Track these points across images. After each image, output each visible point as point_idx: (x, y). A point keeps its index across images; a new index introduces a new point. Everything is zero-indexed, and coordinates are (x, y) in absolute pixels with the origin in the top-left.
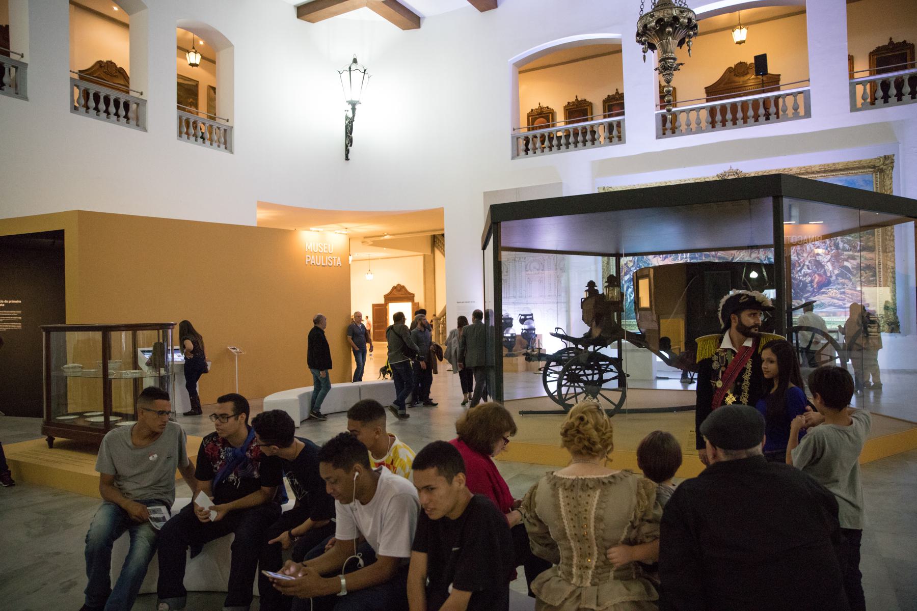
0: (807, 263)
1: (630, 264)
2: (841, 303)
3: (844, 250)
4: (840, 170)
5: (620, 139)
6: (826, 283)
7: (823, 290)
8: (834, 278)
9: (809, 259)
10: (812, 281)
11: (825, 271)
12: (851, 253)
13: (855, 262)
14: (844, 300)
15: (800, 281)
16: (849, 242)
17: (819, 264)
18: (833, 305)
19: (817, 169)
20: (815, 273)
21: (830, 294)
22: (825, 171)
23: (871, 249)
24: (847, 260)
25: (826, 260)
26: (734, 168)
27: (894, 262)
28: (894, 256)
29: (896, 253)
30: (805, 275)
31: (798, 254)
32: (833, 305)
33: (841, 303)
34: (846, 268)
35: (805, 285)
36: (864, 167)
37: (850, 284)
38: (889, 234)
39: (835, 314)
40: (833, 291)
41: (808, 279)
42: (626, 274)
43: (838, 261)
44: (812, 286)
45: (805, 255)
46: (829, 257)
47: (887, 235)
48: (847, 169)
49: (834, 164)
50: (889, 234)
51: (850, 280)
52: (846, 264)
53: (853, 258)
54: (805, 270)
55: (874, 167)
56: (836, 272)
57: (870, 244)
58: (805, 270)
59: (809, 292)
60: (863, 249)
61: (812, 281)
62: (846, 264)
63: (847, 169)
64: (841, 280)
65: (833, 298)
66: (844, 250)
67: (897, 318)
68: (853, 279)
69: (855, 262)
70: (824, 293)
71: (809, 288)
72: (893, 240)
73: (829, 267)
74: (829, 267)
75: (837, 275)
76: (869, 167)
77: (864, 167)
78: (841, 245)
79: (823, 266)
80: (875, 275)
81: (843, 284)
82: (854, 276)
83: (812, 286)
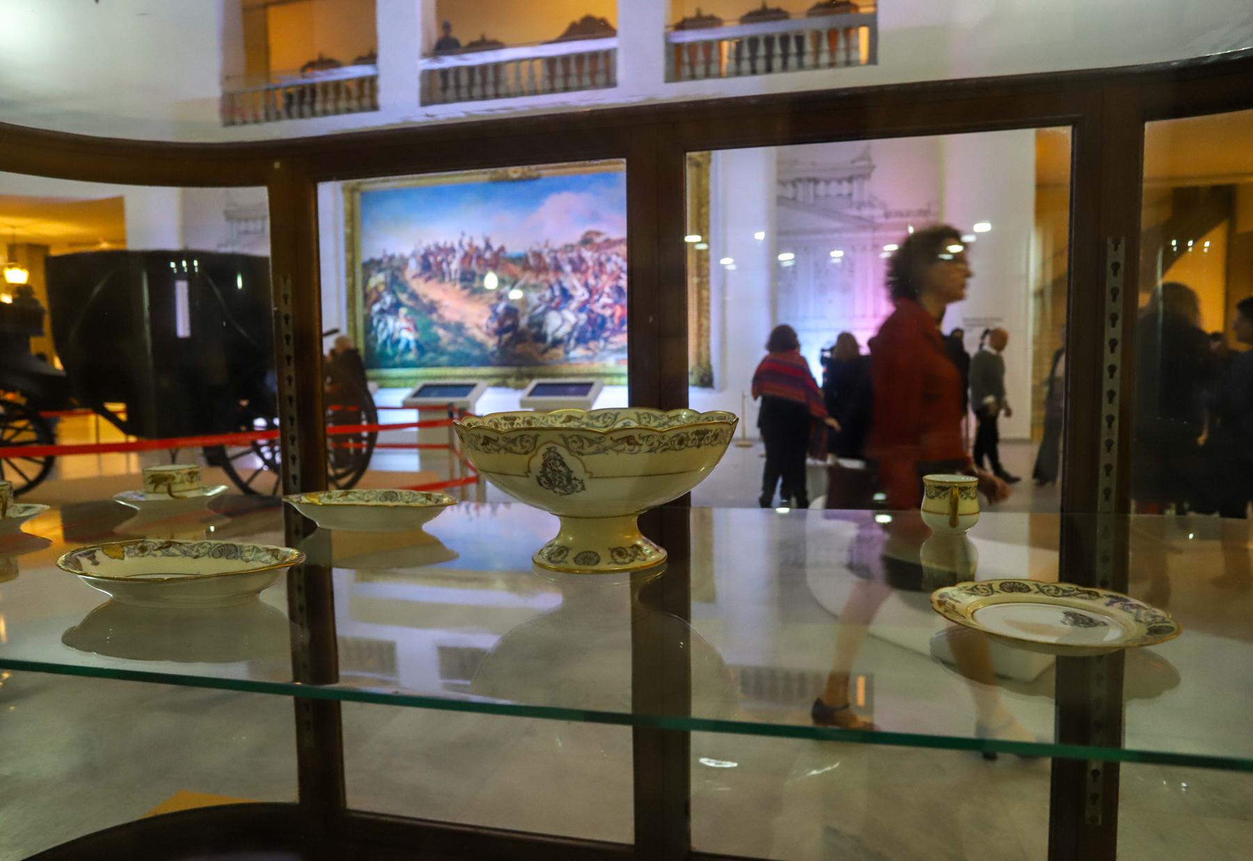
1: (382, 288)
15: (598, 315)
30: (604, 307)
31: (596, 277)
35: (604, 319)
41: (608, 312)
42: (375, 302)
45: (604, 277)
54: (605, 300)
58: (605, 300)
61: (612, 316)
71: (609, 325)
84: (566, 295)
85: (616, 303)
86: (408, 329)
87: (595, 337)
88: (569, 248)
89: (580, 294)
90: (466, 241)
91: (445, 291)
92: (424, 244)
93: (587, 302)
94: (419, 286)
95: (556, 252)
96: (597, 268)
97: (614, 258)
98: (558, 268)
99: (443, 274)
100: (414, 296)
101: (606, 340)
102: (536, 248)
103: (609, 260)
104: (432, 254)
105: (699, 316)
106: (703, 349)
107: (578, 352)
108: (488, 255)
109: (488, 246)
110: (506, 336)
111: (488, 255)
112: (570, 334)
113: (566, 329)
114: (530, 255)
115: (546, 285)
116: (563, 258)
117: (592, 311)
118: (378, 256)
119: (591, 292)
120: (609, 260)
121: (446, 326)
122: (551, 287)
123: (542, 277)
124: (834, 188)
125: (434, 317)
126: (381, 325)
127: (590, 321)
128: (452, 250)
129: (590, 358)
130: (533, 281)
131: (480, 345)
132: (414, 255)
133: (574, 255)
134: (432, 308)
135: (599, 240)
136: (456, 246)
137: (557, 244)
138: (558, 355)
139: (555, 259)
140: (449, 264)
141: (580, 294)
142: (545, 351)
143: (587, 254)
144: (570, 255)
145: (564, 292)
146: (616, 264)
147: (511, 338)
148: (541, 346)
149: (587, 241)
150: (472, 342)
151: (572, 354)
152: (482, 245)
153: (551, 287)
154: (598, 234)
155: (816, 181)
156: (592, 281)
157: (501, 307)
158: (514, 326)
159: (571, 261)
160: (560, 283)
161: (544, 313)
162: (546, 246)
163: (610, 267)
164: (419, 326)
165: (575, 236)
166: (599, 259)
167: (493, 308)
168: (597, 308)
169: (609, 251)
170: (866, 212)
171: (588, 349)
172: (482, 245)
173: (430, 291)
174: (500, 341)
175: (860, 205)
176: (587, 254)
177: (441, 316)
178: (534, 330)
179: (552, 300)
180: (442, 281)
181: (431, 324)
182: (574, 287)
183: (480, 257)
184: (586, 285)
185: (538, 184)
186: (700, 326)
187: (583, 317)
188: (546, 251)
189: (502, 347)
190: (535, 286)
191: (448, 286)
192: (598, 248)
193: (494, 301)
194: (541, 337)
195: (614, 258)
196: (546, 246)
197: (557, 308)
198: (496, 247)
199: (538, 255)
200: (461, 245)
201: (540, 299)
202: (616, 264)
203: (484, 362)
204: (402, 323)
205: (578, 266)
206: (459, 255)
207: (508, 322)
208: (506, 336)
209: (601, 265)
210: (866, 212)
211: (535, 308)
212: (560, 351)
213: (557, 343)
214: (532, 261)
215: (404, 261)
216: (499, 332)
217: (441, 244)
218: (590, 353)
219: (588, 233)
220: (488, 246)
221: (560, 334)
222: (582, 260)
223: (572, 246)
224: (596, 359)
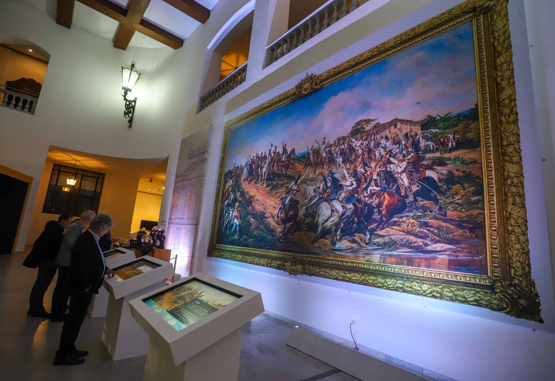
0: (375, 177)
2: (420, 242)
3: (427, 150)
4: (422, 33)
6: (398, 208)
7: (395, 219)
8: (411, 198)
9: (378, 170)
10: (380, 205)
11: (398, 188)
12: (438, 155)
13: (444, 170)
14: (424, 237)
15: (366, 204)
16: (434, 138)
17: (390, 178)
18: (408, 245)
19: (392, 43)
20: (384, 190)
21: (404, 226)
22: (402, 43)
23: (471, 144)
24: (430, 168)
25: (400, 170)
26: (310, 74)
27: (519, 163)
28: (518, 151)
29: (523, 145)
30: (371, 195)
31: (365, 165)
32: (408, 245)
33: (420, 242)
34: (430, 180)
36: (457, 16)
37: (436, 209)
38: (507, 111)
39: (410, 262)
40: (408, 220)
41: (375, 201)
43: (418, 171)
44: (380, 213)
46: (404, 165)
47: (502, 113)
48: (431, 29)
49: (413, 29)
50: (507, 111)
51: (436, 202)
52: (429, 173)
53: (441, 163)
54: (373, 188)
55: (474, 9)
56: (415, 188)
57: (471, 135)
58: (373, 188)
59: (375, 221)
60: (459, 145)
61: (380, 205)
62: (429, 173)
63: (431, 29)
64: (422, 202)
65: (408, 233)
66: (427, 150)
67: (532, 284)
68: (442, 200)
69: (444, 170)
70: (395, 224)
71: (376, 216)
72: (516, 121)
74: (405, 180)
75: (416, 194)
76: (465, 13)
77: (457, 16)
78: (423, 143)
79: (395, 180)
80: (479, 192)
81: (425, 209)
82: (443, 193)
83: (380, 213)
84: (337, 186)
85: (384, 190)
87: (361, 230)
89: (349, 183)
90: (273, 149)
93: (355, 191)
96: (366, 156)
97: (383, 142)
98: (332, 161)
100: (243, 194)
101: (372, 232)
102: (316, 146)
103: (378, 145)
105: (503, 203)
106: (515, 250)
107: (344, 244)
109: (285, 150)
110: (288, 225)
112: (337, 224)
113: (335, 219)
115: (321, 178)
117: (359, 201)
118: (232, 168)
119: (359, 181)
120: (378, 145)
121: (254, 216)
122: (325, 180)
126: (227, 214)
127: (356, 212)
129: (354, 251)
130: (311, 176)
131: (272, 231)
132: (246, 165)
135: (368, 128)
138: (325, 245)
139: (330, 152)
140: (262, 168)
141: (349, 183)
142: (316, 240)
144: (342, 147)
145: (335, 181)
146: (385, 148)
147: (292, 226)
148: (312, 234)
149: (357, 131)
150: (267, 226)
151: (338, 246)
154: (368, 121)
156: (360, 170)
158: (295, 215)
159: (343, 153)
160: (333, 174)
161: (317, 204)
162: (324, 143)
165: (347, 128)
167: (283, 199)
168: (364, 197)
169: (378, 137)
171: (354, 241)
174: (285, 229)
176: (356, 144)
177: (253, 208)
178: (308, 221)
179: (325, 191)
182: (344, 177)
183: (279, 160)
184: (355, 174)
185: (322, 92)
186: (505, 218)
187: (350, 206)
189: (285, 233)
190: (312, 180)
193: (284, 196)
194: (313, 227)
195: (383, 142)
196: (324, 143)
197: (329, 200)
199: (317, 152)
200: (270, 153)
201: (315, 191)
202: (385, 148)
203: (272, 246)
204: (235, 214)
205: (348, 156)
207: (291, 213)
208: (288, 225)
209: (370, 151)
211: (311, 200)
212: (328, 242)
213: (326, 232)
215: (242, 169)
216: (284, 221)
218: (354, 245)
219: (358, 123)
220: (285, 150)
221: (329, 224)
222: (352, 149)
223: (344, 138)
224: (361, 254)
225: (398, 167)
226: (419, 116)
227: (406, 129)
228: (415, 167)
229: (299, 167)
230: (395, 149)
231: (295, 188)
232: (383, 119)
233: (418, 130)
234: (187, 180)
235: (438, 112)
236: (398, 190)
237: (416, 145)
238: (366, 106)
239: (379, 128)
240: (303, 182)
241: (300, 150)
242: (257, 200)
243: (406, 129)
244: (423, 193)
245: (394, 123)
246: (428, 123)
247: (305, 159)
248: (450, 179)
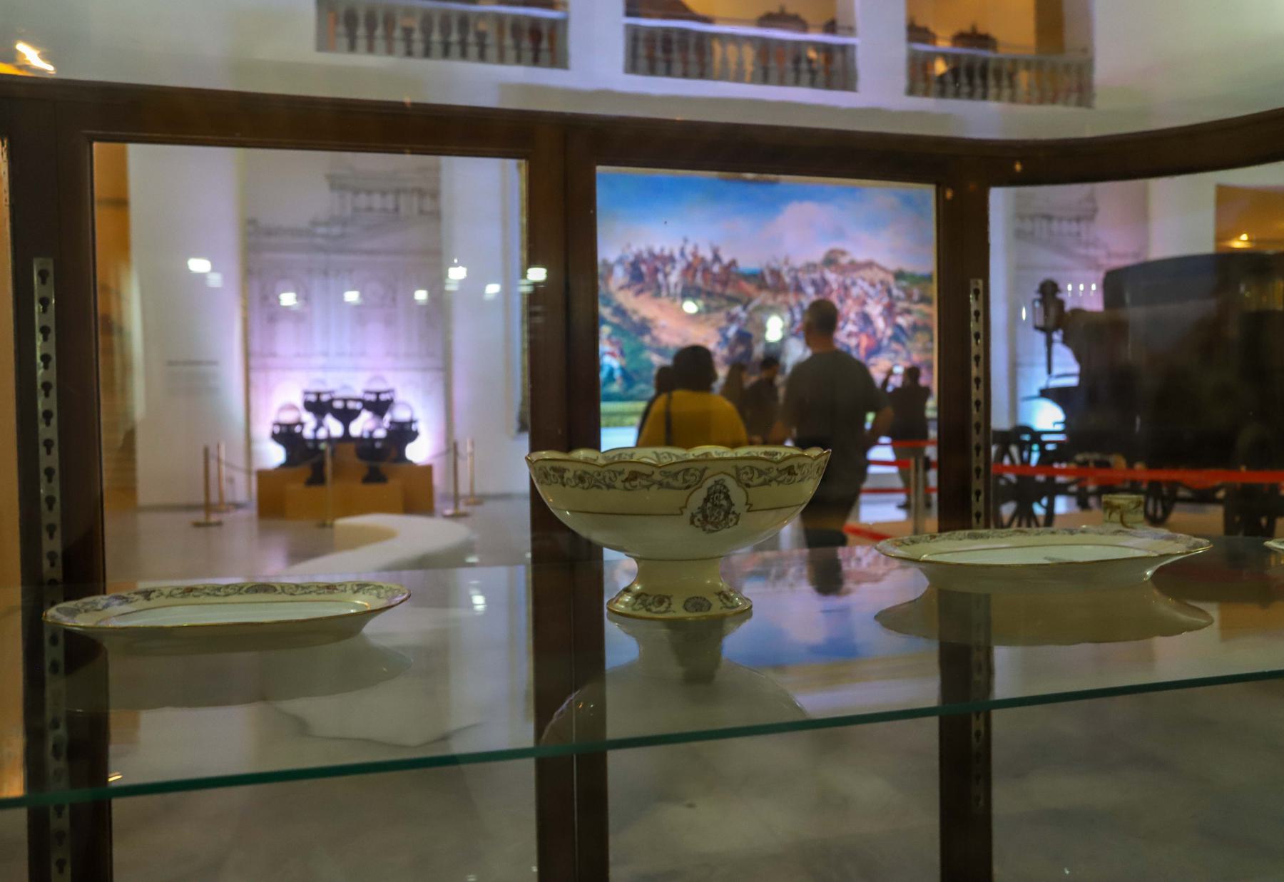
3: (898, 299)
5: (558, 59)
16: (904, 289)
17: (866, 319)
30: (850, 335)
34: (899, 327)
45: (849, 302)
51: (903, 344)
53: (907, 312)
54: (851, 327)
58: (851, 327)
61: (858, 346)
64: (894, 346)
68: (909, 345)
73: (880, 323)
74: (880, 323)
78: (895, 292)
85: (861, 331)
86: (612, 354)
88: (811, 267)
90: (689, 249)
91: (661, 307)
92: (635, 249)
94: (627, 299)
95: (797, 270)
96: (842, 292)
97: (860, 282)
99: (659, 287)
100: (620, 311)
102: (774, 265)
103: (854, 283)
104: (644, 261)
108: (716, 268)
109: (717, 258)
111: (716, 268)
114: (767, 273)
116: (805, 278)
120: (854, 283)
123: (780, 298)
124: (1067, 227)
125: (647, 339)
128: (671, 259)
132: (620, 261)
133: (816, 276)
134: (644, 327)
135: (844, 260)
136: (677, 255)
137: (798, 262)
139: (796, 279)
140: (666, 275)
143: (831, 276)
146: (862, 288)
149: (831, 261)
152: (708, 256)
153: (791, 310)
154: (843, 253)
155: (1049, 218)
157: (732, 331)
159: (814, 283)
162: (786, 263)
163: (855, 291)
164: (627, 350)
166: (844, 282)
169: (855, 275)
170: (1092, 252)
172: (708, 256)
173: (643, 307)
175: (1087, 245)
176: (831, 276)
177: (654, 339)
180: (657, 295)
181: (642, 348)
183: (706, 270)
188: (784, 270)
191: (665, 301)
192: (842, 270)
193: (724, 323)
195: (860, 282)
196: (786, 263)
198: (726, 259)
199: (776, 274)
200: (682, 254)
206: (680, 265)
210: (1092, 252)
214: (769, 280)
217: (657, 250)
219: (832, 252)
222: (825, 282)
225: (875, 310)
226: (893, 266)
227: (881, 275)
228: (890, 311)
229: (750, 288)
230: (871, 291)
231: (743, 315)
232: (860, 257)
233: (890, 279)
234: (341, 251)
235: (908, 267)
236: (875, 333)
237: (889, 292)
238: (840, 233)
239: (855, 266)
240: (760, 308)
241: (748, 263)
242: (664, 327)
243: (881, 275)
244: (894, 338)
245: (869, 265)
246: (899, 275)
247: (757, 278)
248: (915, 327)
